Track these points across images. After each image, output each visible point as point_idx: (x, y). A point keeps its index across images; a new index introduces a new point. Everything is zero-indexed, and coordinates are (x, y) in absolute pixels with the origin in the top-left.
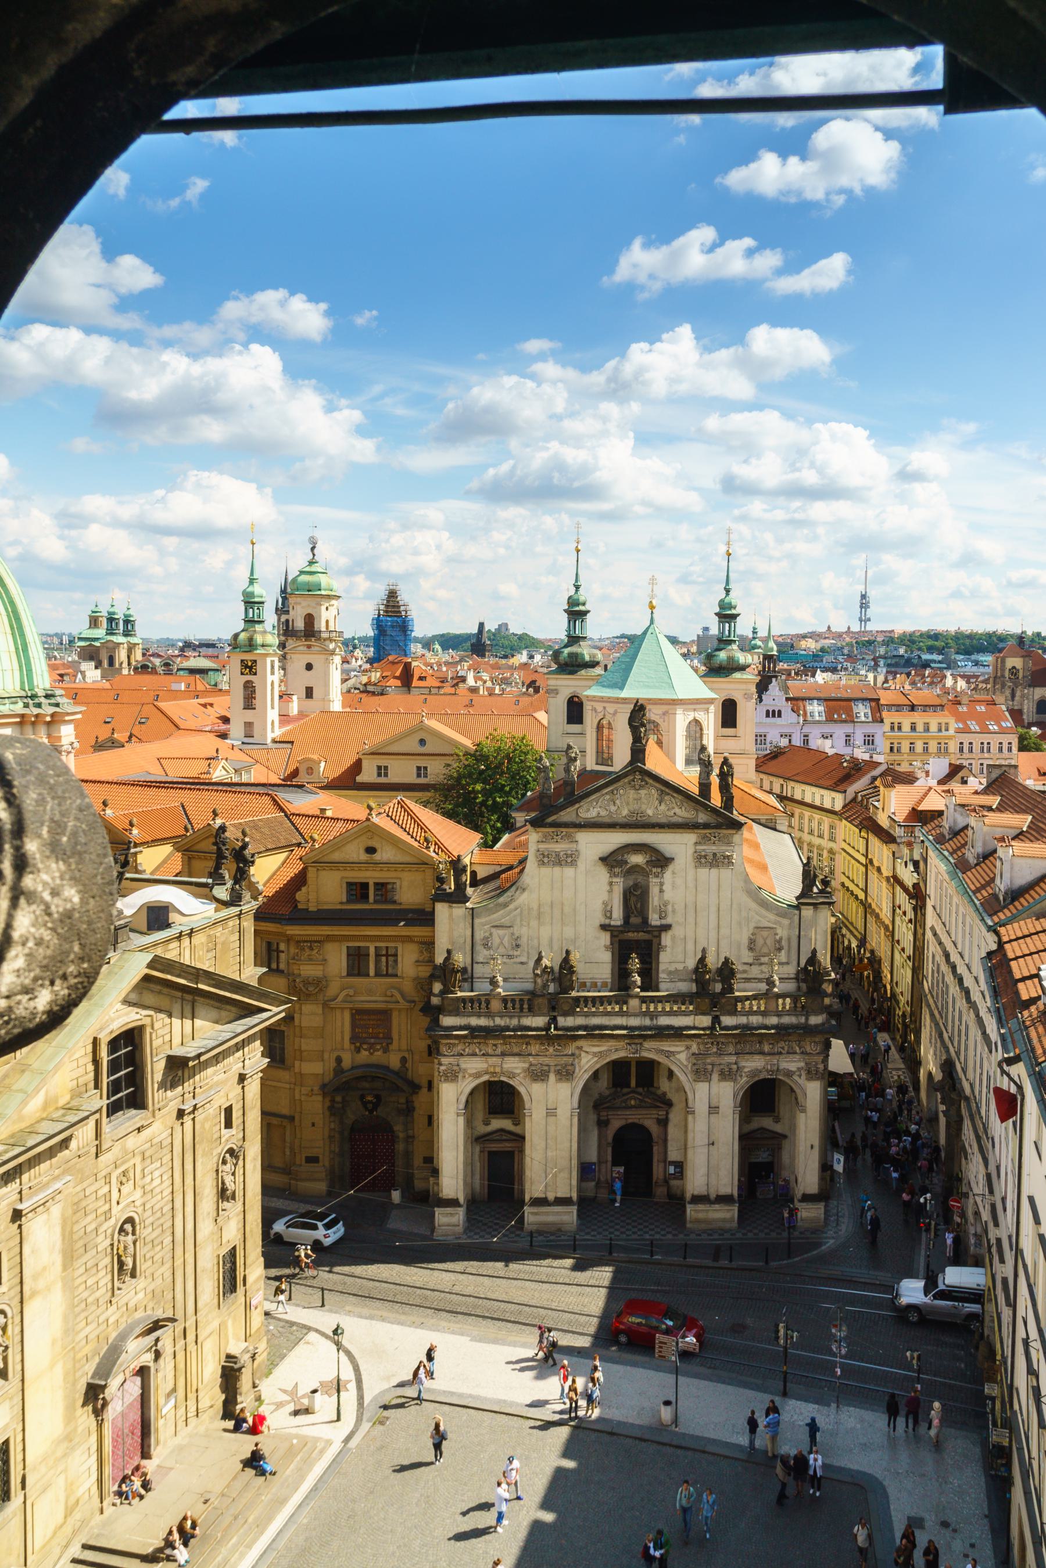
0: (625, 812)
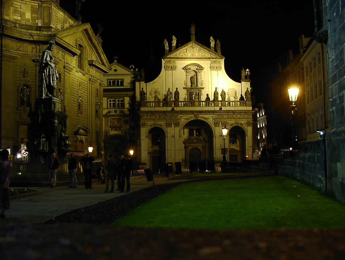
0: (190, 55)
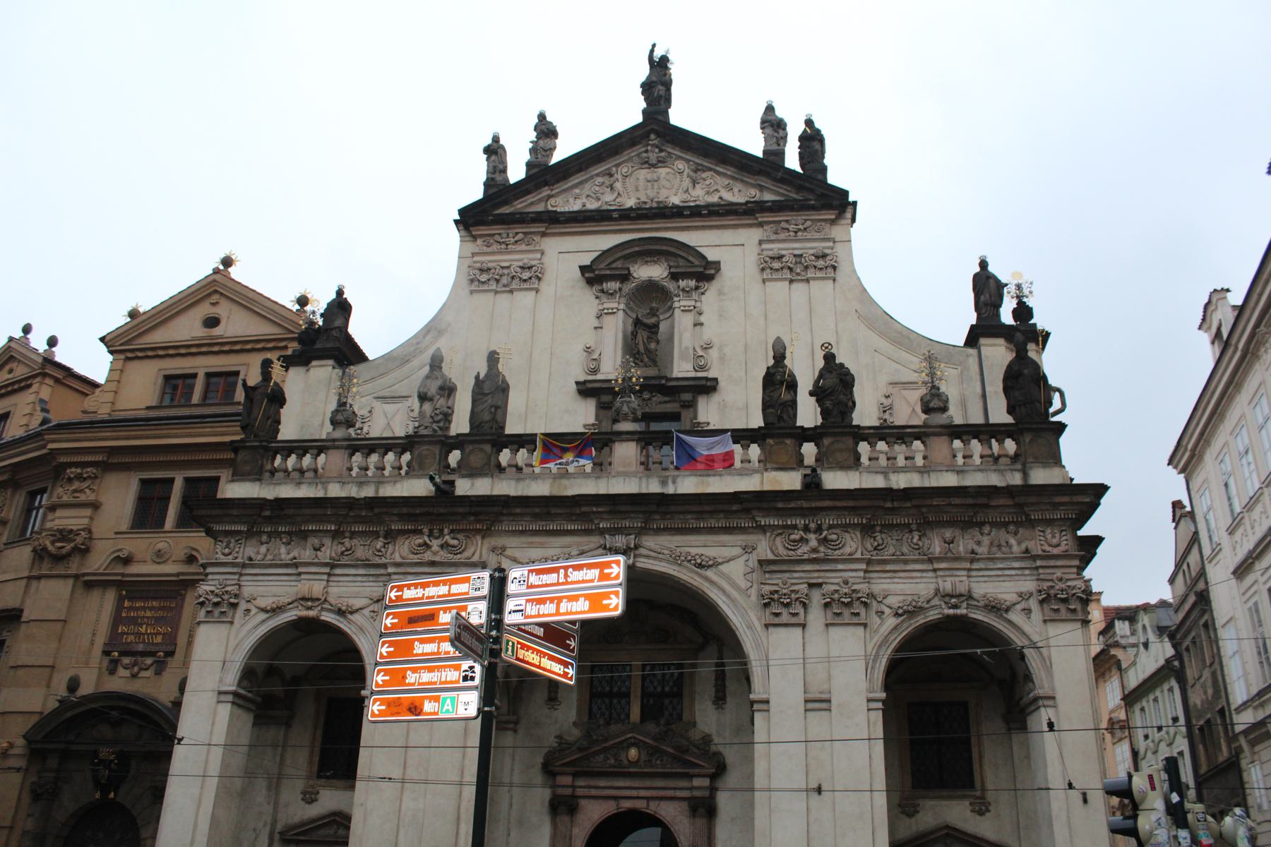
0: (630, 203)
